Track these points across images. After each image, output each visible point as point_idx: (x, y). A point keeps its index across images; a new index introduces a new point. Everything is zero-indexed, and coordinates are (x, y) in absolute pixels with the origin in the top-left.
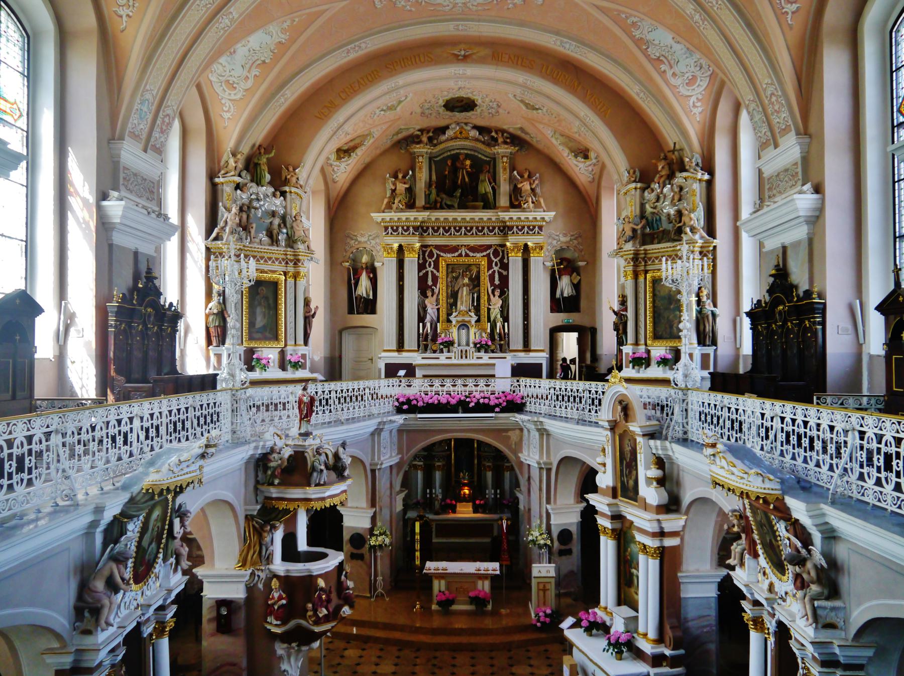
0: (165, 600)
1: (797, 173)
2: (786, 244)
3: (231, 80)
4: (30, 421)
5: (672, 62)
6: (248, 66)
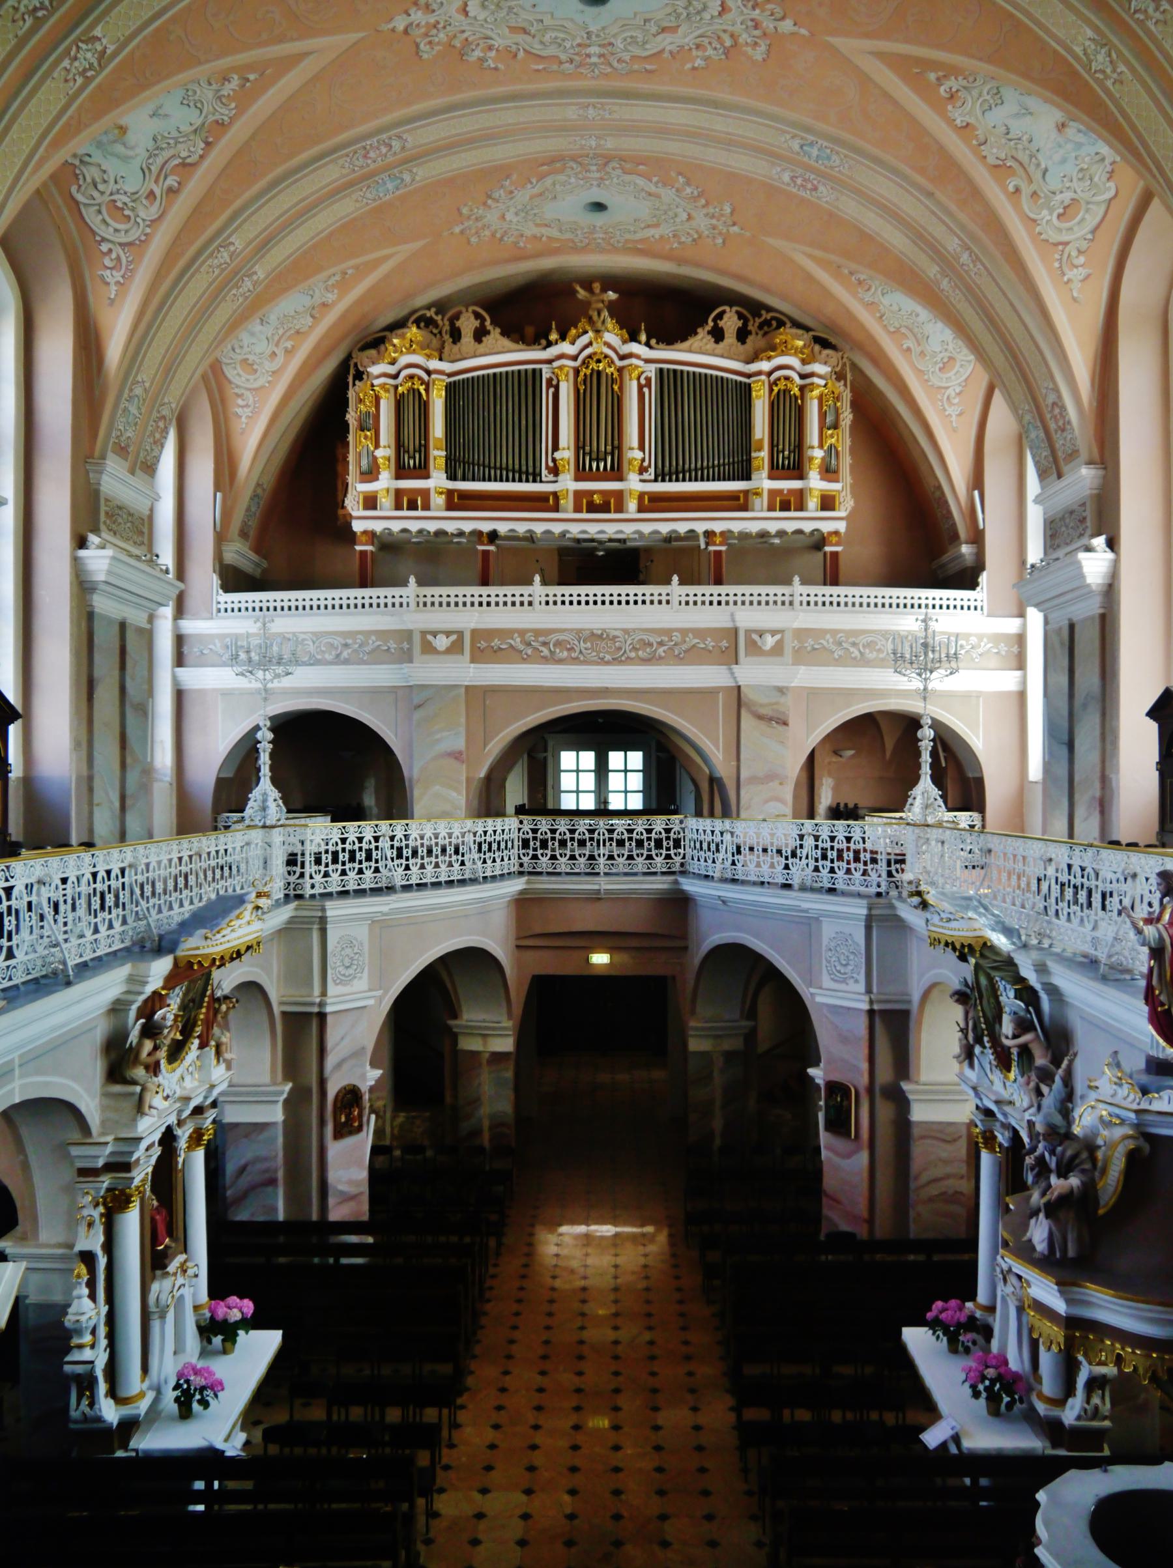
0: (206, 1098)
1: (1085, 518)
2: (1075, 620)
3: (251, 358)
4: (8, 867)
5: (919, 336)
6: (276, 338)
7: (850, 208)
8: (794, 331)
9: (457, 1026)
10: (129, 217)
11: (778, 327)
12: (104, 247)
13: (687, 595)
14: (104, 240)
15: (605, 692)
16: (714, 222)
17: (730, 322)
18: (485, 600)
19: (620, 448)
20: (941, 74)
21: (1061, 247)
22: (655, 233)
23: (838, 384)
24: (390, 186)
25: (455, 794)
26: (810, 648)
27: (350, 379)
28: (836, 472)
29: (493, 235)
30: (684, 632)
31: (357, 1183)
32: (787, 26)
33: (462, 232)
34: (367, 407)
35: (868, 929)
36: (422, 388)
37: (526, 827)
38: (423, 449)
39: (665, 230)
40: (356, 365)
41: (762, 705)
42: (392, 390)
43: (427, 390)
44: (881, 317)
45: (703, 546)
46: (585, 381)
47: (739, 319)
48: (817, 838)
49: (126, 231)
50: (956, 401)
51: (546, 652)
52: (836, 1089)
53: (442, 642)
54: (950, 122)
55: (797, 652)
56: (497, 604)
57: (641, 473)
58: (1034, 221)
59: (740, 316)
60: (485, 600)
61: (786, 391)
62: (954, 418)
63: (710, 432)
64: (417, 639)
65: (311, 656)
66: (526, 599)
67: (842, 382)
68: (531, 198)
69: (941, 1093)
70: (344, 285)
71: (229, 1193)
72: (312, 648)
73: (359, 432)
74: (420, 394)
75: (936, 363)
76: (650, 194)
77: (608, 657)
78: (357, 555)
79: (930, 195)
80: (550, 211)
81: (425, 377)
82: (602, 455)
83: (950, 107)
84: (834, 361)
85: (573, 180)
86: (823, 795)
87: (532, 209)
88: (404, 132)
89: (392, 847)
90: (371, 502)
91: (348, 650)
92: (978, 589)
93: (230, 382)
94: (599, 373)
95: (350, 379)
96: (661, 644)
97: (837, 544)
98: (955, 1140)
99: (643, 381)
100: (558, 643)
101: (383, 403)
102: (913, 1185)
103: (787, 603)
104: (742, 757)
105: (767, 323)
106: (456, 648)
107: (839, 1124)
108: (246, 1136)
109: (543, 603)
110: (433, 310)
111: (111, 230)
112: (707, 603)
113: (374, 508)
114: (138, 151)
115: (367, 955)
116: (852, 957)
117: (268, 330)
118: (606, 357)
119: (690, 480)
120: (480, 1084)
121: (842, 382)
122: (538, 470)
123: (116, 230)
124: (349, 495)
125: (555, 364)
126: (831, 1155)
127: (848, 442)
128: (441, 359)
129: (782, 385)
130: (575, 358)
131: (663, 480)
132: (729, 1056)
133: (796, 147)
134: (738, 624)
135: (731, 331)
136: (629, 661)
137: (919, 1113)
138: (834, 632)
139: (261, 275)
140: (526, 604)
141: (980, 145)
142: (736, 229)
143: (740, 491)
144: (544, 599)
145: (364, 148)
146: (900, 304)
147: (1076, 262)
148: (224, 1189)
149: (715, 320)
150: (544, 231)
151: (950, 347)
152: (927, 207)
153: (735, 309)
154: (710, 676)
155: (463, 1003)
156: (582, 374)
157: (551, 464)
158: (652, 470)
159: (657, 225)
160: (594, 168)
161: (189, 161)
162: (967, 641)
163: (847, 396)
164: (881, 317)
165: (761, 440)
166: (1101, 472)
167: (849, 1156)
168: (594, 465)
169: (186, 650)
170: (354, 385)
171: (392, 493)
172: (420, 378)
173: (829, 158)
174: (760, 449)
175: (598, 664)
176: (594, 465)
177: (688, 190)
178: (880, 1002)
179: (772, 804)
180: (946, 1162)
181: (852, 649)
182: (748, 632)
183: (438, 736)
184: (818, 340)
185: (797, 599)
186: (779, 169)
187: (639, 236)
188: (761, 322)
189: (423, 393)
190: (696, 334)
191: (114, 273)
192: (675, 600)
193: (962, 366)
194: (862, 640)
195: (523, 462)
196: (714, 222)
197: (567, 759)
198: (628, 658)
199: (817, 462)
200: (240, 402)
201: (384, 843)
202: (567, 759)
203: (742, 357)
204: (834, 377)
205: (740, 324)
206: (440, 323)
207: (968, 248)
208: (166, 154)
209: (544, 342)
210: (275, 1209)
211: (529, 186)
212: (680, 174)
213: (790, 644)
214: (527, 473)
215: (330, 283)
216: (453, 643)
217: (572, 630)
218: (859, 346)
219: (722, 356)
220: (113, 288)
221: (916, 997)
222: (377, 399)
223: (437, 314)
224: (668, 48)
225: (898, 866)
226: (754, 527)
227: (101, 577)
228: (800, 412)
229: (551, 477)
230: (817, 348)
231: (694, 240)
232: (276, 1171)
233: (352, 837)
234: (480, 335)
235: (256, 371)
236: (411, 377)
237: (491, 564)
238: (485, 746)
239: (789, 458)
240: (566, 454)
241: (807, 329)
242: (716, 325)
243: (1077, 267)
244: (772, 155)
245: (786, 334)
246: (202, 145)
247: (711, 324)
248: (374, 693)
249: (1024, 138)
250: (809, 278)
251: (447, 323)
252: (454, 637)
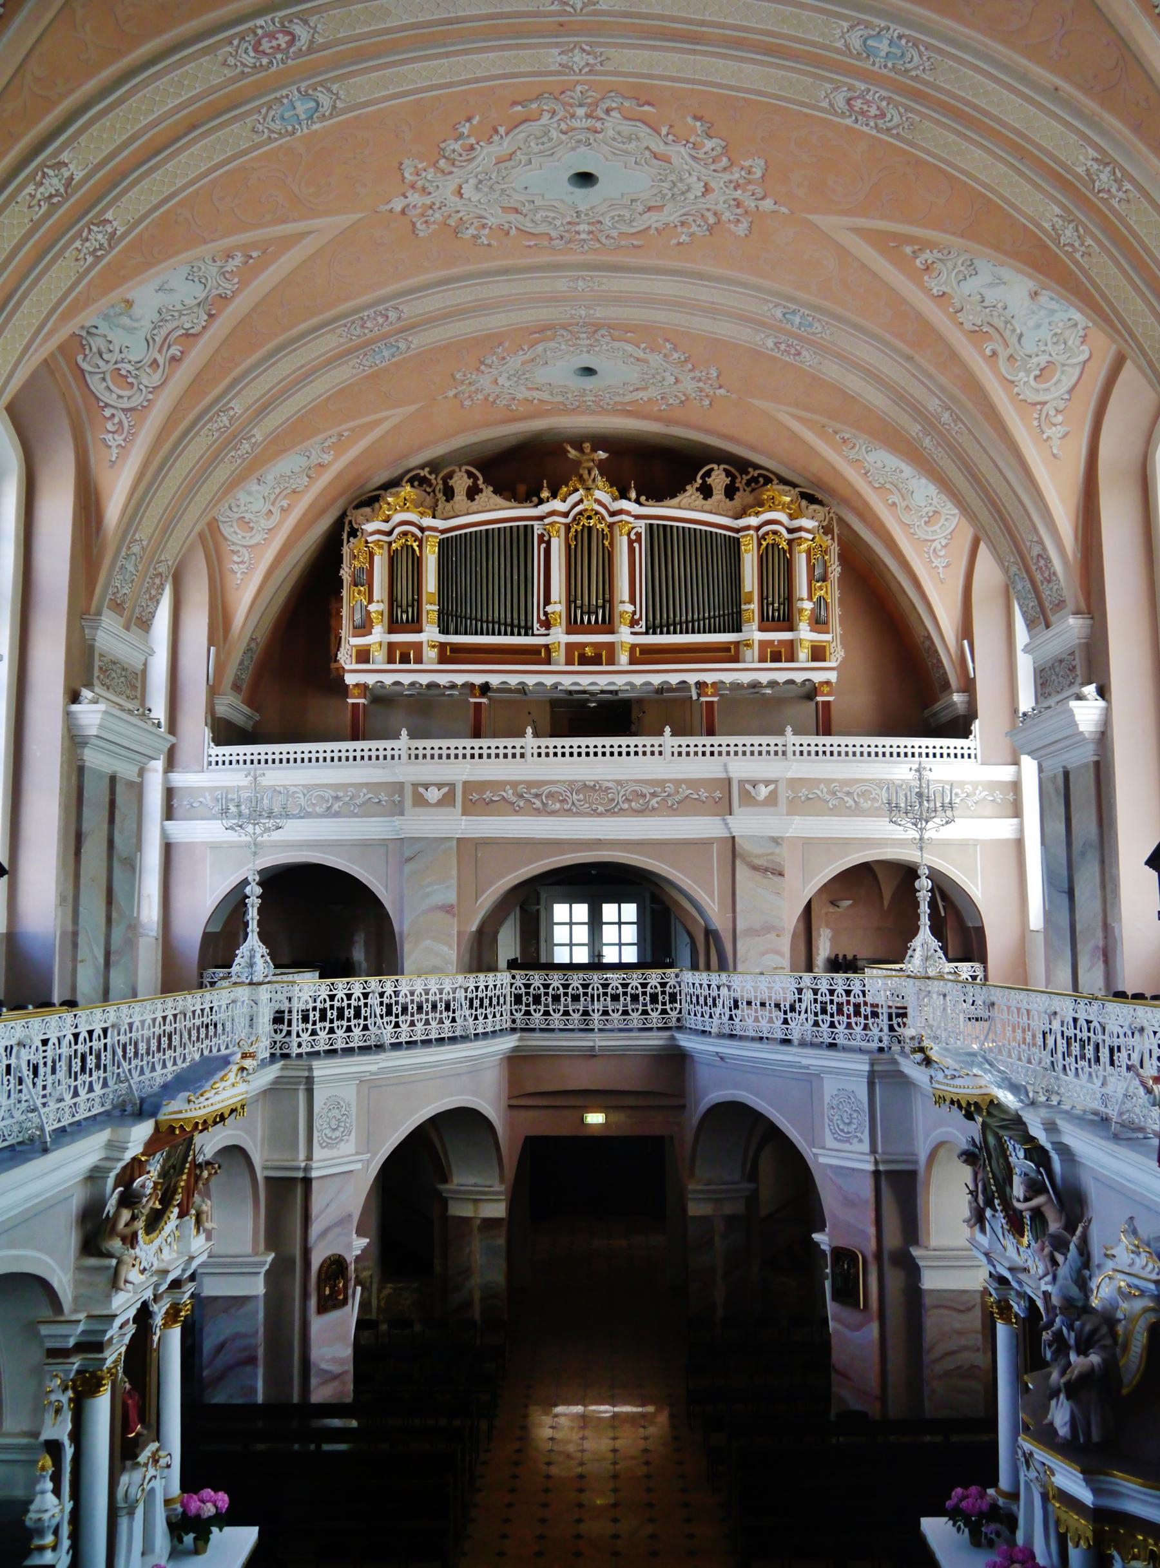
0: (184, 1270)
1: (1074, 667)
3: (248, 516)
6: (273, 497)
7: (832, 371)
8: (782, 487)
9: (449, 1191)
10: (132, 384)
11: (765, 484)
12: (107, 413)
13: (680, 746)
14: (107, 405)
15: (598, 844)
16: (701, 384)
17: (718, 479)
18: (477, 752)
19: (611, 601)
20: (916, 247)
21: (1038, 407)
22: (644, 395)
23: (825, 538)
24: (386, 353)
25: (446, 949)
26: (805, 798)
27: (345, 537)
28: (826, 623)
29: (486, 399)
30: (677, 783)
31: (341, 1362)
32: (768, 205)
33: (455, 396)
34: (361, 562)
35: (871, 1085)
36: (415, 545)
37: (519, 982)
38: (417, 603)
39: (653, 393)
40: (350, 522)
41: (757, 856)
42: (386, 546)
43: (420, 546)
44: (866, 474)
45: (695, 697)
46: (576, 537)
47: (727, 476)
48: (815, 992)
49: (129, 398)
50: (942, 553)
51: (538, 804)
52: (842, 1255)
53: (433, 795)
54: (928, 292)
55: (791, 801)
56: (489, 756)
57: (632, 626)
58: (1013, 382)
59: (728, 473)
60: (477, 752)
61: (775, 545)
62: (941, 570)
63: (699, 586)
64: (408, 791)
65: (302, 809)
66: (518, 751)
67: (830, 536)
68: (523, 363)
69: (953, 1260)
70: (340, 446)
71: (205, 1373)
72: (302, 801)
73: (353, 588)
74: (413, 550)
75: (921, 517)
76: (638, 360)
77: (601, 809)
78: (350, 708)
79: (910, 359)
80: (542, 375)
81: (419, 534)
82: (593, 609)
83: (926, 278)
84: (821, 516)
85: (563, 347)
86: (821, 947)
88: (401, 303)
89: (382, 1003)
90: (363, 656)
91: (339, 802)
92: (971, 737)
93: (226, 539)
94: (590, 528)
95: (345, 537)
96: (654, 795)
97: (828, 695)
98: (969, 1309)
99: (633, 537)
100: (550, 795)
101: (377, 559)
102: (926, 1359)
103: (780, 753)
104: (738, 908)
105: (754, 480)
106: (448, 800)
107: (847, 1293)
108: (225, 1311)
109: (535, 755)
110: (427, 469)
111: (115, 396)
112: (700, 754)
113: (367, 661)
114: (143, 323)
115: (354, 1117)
116: (855, 1115)
117: (265, 490)
118: (597, 513)
119: (681, 632)
120: (470, 1253)
121: (830, 536)
122: (529, 624)
123: (120, 397)
124: (342, 649)
125: (547, 521)
126: (839, 1327)
127: (837, 594)
128: (434, 517)
129: (770, 539)
130: (566, 515)
131: (654, 633)
132: (730, 1220)
133: (780, 316)
134: (731, 775)
135: (719, 487)
136: (622, 812)
137: (931, 1281)
138: (828, 782)
139: (259, 437)
140: (518, 756)
141: (956, 312)
142: (722, 391)
143: (731, 643)
144: (536, 751)
145: (362, 318)
146: (884, 460)
147: (1054, 420)
148: (201, 1369)
149: (703, 478)
150: (536, 394)
151: (935, 502)
152: (906, 369)
153: (722, 466)
154: (702, 827)
155: (452, 1162)
156: (573, 530)
157: (542, 618)
158: (643, 623)
159: (645, 389)
160: (584, 336)
161: (191, 331)
162: (962, 789)
163: (835, 549)
164: (866, 474)
165: (751, 593)
166: (1088, 622)
167: (858, 1328)
168: (586, 618)
169: (175, 802)
170: (348, 541)
171: (385, 647)
172: (413, 535)
173: (811, 326)
174: (750, 602)
175: (591, 815)
176: (586, 618)
177: (676, 356)
178: (885, 1162)
179: (770, 956)
180: (959, 1333)
181: (846, 799)
182: (741, 782)
183: (429, 890)
184: (804, 496)
185: (790, 749)
186: (763, 336)
187: (627, 399)
188: (748, 479)
189: (417, 549)
190: (685, 491)
191: (116, 436)
192: (667, 751)
193: (946, 520)
194: (856, 789)
195: (515, 616)
196: (701, 384)
197: (560, 911)
198: (621, 809)
199: (807, 613)
200: (236, 558)
201: (374, 1000)
202: (560, 911)
203: (730, 513)
204: (821, 531)
205: (728, 481)
206: (434, 482)
207: (950, 409)
208: (170, 326)
209: (535, 499)
210: (254, 1390)
211: (521, 353)
212: (667, 340)
213: (784, 794)
214: (519, 627)
215: (326, 445)
216: (444, 795)
217: (565, 782)
218: (845, 502)
219: (711, 512)
220: (115, 451)
221: (923, 1157)
222: (371, 555)
223: (430, 473)
224: (654, 225)
225: (900, 1020)
226: (745, 678)
227: (93, 731)
228: (789, 565)
229: (543, 631)
230: (804, 503)
231: (682, 402)
232: (255, 1348)
233: (340, 994)
234: (472, 493)
235: (252, 528)
236: (405, 534)
237: (483, 716)
238: (477, 900)
239: (779, 610)
240: (558, 608)
241: (794, 485)
242: (704, 482)
243: (1055, 425)
244: (758, 323)
245: (774, 490)
246: (206, 317)
247: (699, 481)
248: (365, 846)
249: (999, 305)
250: (795, 438)
251: (441, 482)
252: (445, 790)
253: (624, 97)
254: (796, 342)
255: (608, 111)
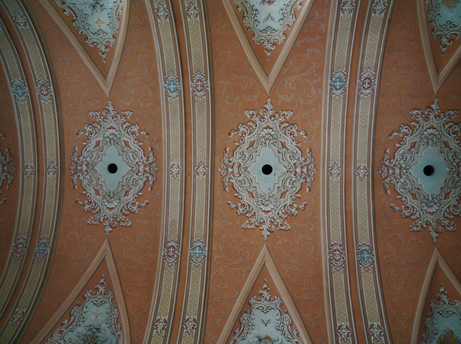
20: (266, 52)
24: (366, 255)
29: (450, 219)
32: (269, 106)
54: (285, 41)
83: (279, 43)
85: (402, 180)
87: (428, 199)
114: (280, 338)
141: (290, 26)
142: (434, 106)
160: (391, 171)
161: (290, 323)
186: (361, 95)
208: (286, 329)
215: (447, 302)
224: (295, 144)
246: (287, 315)
249: (282, 12)
253: (223, 157)
254: (358, 81)
255: (230, 162)
